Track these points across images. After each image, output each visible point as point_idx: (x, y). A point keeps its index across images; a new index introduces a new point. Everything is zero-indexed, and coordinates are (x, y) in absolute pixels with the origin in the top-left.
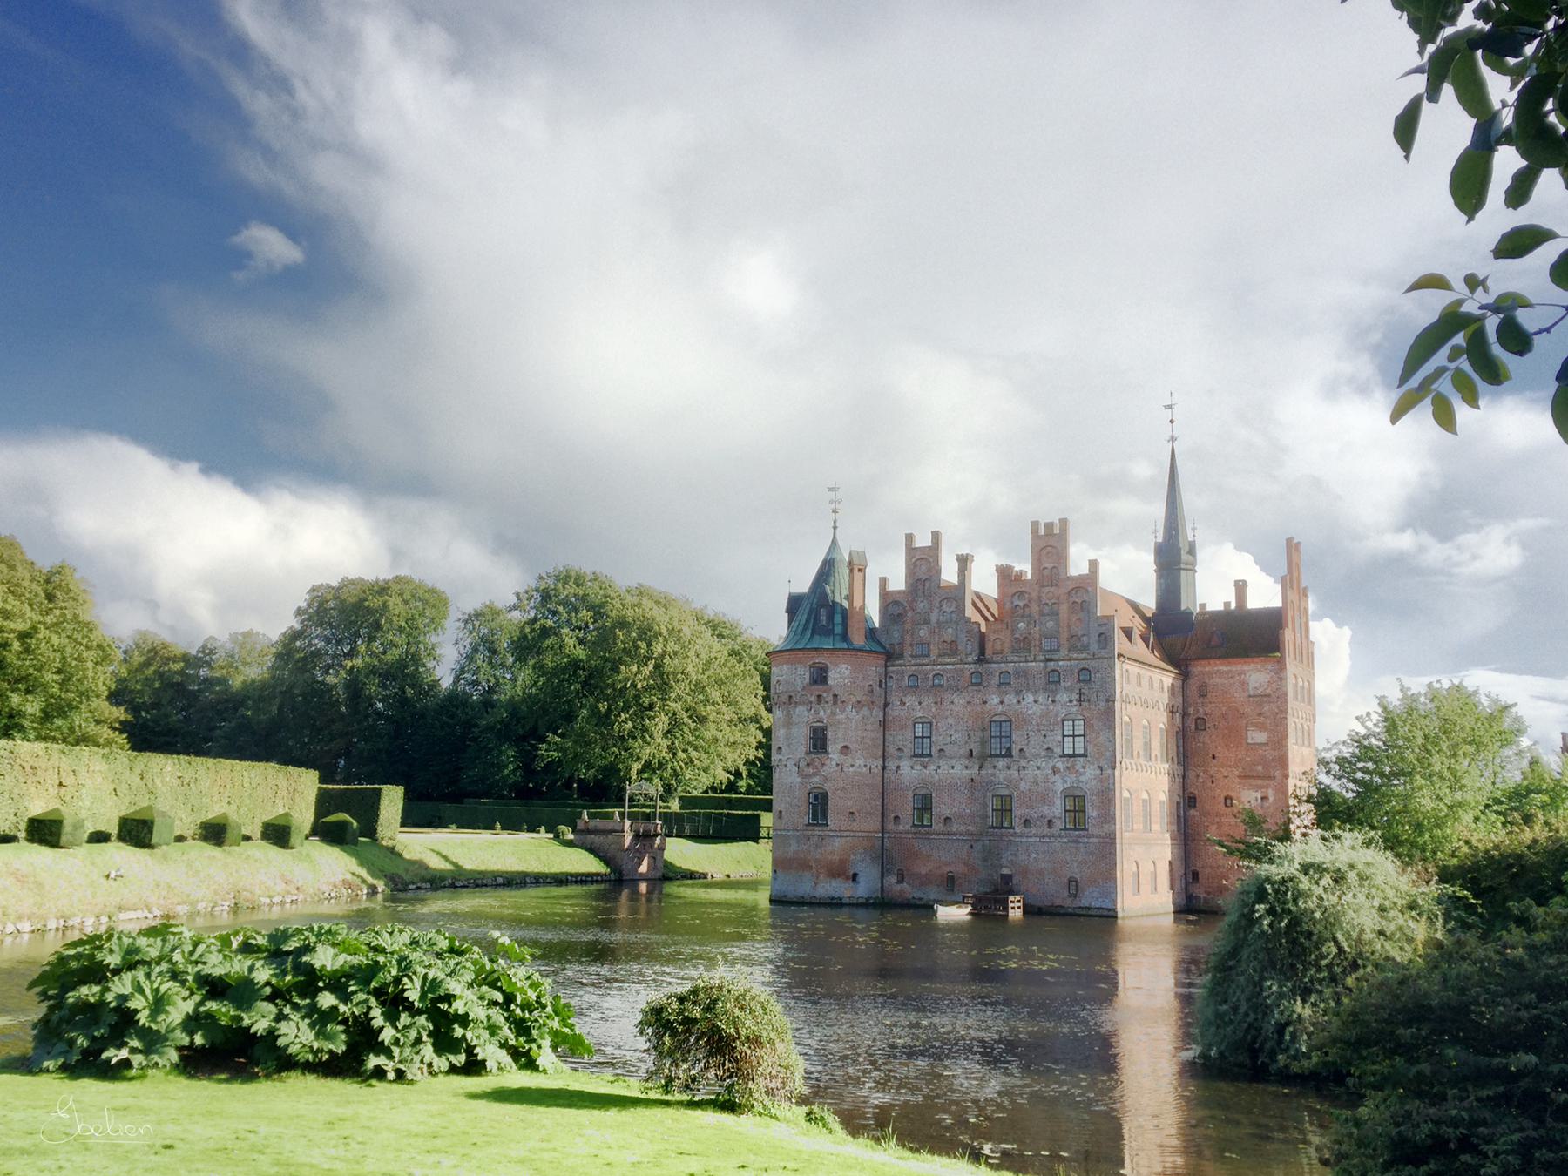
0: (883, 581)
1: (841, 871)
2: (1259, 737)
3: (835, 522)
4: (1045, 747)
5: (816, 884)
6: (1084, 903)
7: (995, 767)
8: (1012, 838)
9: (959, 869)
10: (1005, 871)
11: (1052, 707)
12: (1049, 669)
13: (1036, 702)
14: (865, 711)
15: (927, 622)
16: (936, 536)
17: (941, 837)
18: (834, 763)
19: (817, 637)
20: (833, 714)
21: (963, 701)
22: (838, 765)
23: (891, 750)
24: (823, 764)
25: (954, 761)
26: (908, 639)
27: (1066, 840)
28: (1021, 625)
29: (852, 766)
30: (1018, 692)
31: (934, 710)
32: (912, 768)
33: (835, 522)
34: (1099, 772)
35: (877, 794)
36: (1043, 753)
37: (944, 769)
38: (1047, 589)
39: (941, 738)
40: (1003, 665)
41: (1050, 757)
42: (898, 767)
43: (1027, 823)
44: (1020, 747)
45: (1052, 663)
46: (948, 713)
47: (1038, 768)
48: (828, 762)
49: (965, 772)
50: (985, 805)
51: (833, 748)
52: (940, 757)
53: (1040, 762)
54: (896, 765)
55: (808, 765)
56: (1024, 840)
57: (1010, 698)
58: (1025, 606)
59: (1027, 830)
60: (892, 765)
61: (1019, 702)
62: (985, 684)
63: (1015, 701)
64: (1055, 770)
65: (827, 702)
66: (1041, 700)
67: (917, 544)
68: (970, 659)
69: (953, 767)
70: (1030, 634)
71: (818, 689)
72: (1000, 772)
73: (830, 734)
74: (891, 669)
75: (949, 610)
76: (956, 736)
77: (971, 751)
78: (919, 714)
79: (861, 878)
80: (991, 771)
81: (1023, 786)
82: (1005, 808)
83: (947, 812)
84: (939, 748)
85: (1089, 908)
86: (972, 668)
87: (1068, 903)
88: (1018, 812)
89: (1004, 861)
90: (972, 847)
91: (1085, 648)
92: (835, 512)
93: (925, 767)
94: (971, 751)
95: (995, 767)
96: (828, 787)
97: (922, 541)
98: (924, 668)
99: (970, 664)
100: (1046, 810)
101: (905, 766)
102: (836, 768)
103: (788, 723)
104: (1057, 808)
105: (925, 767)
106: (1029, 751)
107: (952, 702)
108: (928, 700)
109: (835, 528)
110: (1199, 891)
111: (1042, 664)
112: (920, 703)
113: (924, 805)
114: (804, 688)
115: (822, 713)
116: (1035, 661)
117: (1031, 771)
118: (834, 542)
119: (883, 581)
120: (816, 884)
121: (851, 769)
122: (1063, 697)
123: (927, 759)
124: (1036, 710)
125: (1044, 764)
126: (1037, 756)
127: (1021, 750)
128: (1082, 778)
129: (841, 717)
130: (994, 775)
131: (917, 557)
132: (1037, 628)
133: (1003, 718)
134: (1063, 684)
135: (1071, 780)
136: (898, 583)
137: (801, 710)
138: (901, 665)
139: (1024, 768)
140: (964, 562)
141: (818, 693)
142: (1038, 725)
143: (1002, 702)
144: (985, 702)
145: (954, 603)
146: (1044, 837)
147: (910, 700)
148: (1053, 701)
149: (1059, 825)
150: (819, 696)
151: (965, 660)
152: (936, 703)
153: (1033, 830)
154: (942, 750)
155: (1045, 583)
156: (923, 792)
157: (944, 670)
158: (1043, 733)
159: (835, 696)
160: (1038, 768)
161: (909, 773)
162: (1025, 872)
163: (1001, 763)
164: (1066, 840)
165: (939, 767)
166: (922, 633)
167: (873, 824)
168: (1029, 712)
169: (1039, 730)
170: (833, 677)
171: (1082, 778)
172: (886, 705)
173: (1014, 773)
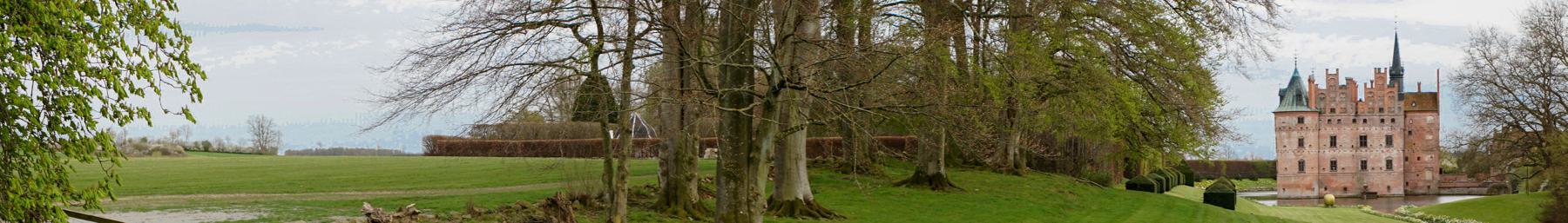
1: (1310, 188)
2: (1430, 137)
6: (1392, 193)
9: (1348, 185)
15: (1334, 101)
16: (1337, 70)
23: (1321, 145)
35: (1317, 160)
43: (1373, 169)
50: (1357, 164)
51: (1306, 146)
57: (1367, 128)
60: (1321, 151)
64: (1383, 151)
71: (1301, 125)
72: (1363, 152)
73: (1305, 141)
82: (1364, 165)
83: (1342, 166)
87: (1388, 194)
88: (1369, 165)
96: (1305, 159)
103: (1289, 137)
104: (1384, 164)
106: (1374, 145)
110: (1409, 189)
113: (1334, 164)
117: (1375, 152)
118: (1296, 71)
122: (1385, 128)
124: (1376, 132)
135: (1388, 155)
137: (1295, 132)
149: (1384, 169)
161: (1329, 153)
162: (1372, 184)
163: (1364, 149)
167: (1316, 171)
170: (1306, 121)
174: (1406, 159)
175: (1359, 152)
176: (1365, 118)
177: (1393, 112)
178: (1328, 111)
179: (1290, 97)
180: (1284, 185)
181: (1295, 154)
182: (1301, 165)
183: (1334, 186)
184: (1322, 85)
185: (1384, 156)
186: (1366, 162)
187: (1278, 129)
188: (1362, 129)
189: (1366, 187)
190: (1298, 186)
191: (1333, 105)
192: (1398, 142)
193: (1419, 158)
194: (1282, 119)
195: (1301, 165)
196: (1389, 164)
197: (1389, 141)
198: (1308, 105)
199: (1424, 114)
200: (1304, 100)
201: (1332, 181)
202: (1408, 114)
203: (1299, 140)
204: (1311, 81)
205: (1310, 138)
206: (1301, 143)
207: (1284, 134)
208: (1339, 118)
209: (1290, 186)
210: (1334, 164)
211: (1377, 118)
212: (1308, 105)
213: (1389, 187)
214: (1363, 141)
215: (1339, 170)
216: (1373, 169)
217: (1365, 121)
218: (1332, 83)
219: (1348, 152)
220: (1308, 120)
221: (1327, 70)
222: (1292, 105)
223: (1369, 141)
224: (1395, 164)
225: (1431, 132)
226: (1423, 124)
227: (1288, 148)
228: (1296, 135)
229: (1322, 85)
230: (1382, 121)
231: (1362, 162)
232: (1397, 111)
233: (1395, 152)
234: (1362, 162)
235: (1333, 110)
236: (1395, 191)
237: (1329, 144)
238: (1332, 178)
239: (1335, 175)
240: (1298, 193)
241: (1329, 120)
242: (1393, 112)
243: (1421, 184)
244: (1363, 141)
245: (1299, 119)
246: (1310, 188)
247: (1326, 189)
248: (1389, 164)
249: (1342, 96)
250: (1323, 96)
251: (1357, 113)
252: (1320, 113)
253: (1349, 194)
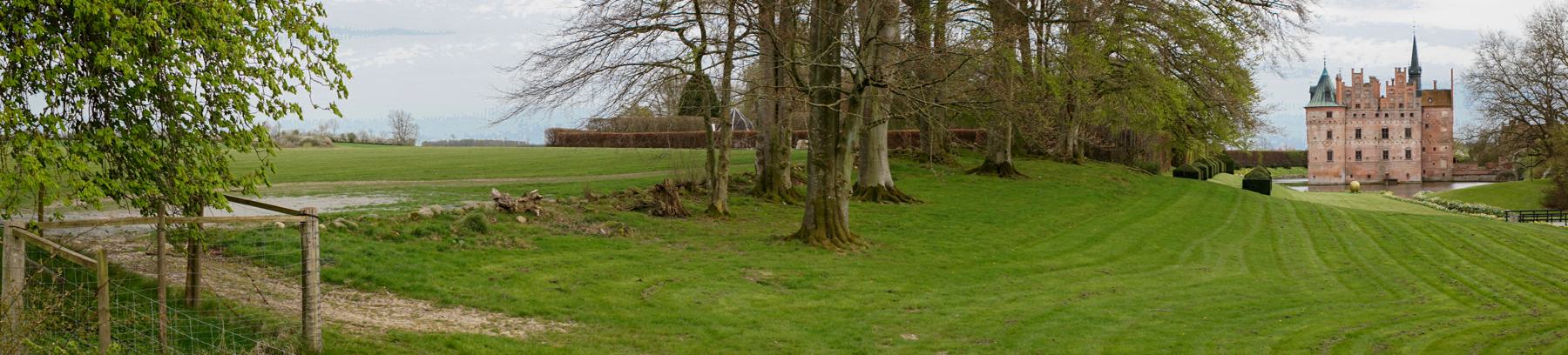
1: (1337, 175)
2: (1445, 130)
9: (1371, 173)
23: (1348, 137)
35: (1343, 151)
43: (1394, 158)
51: (1334, 137)
57: (1388, 122)
60: (1348, 142)
67: (1355, 72)
71: (1330, 119)
72: (1385, 144)
73: (1333, 133)
82: (1386, 155)
83: (1367, 156)
87: (1407, 181)
88: (1390, 155)
91: (1412, 107)
96: (1333, 149)
97: (1357, 71)
101: (1353, 143)
103: (1319, 130)
104: (1404, 154)
106: (1395, 137)
108: (1361, 122)
110: (1426, 176)
113: (1359, 154)
118: (1325, 70)
122: (1405, 122)
124: (1397, 125)
137: (1324, 126)
149: (1404, 158)
161: (1355, 144)
162: (1393, 172)
163: (1385, 141)
167: (1343, 160)
174: (1423, 149)
177: (1412, 107)
178: (1354, 106)
179: (1319, 94)
180: (1314, 173)
182: (1330, 155)
184: (1349, 84)
185: (1404, 147)
187: (1309, 123)
188: (1384, 123)
189: (1387, 175)
190: (1327, 174)
191: (1358, 101)
192: (1416, 134)
193: (1435, 149)
194: (1312, 113)
195: (1330, 155)
196: (1408, 153)
197: (1408, 133)
198: (1335, 101)
199: (1438, 109)
200: (1332, 96)
201: (1356, 169)
202: (1425, 109)
203: (1328, 132)
204: (1338, 79)
205: (1338, 130)
206: (1329, 135)
207: (1314, 127)
209: (1319, 174)
210: (1359, 154)
211: (1397, 113)
212: (1335, 101)
214: (1385, 133)
215: (1363, 160)
216: (1394, 158)
217: (1387, 115)
218: (1357, 81)
220: (1336, 114)
221: (1353, 70)
223: (1390, 133)
224: (1413, 154)
225: (1445, 126)
226: (1438, 118)
227: (1318, 140)
228: (1325, 128)
229: (1349, 84)
230: (1402, 115)
231: (1384, 152)
232: (1415, 107)
233: (1414, 143)
234: (1384, 152)
235: (1358, 106)
236: (1413, 179)
237: (1354, 136)
238: (1357, 166)
239: (1360, 164)
240: (1327, 180)
241: (1355, 115)
243: (1436, 172)
244: (1385, 133)
245: (1328, 113)
246: (1337, 175)
247: (1352, 176)
248: (1408, 153)
250: (1348, 93)
251: (1379, 108)
252: (1347, 108)
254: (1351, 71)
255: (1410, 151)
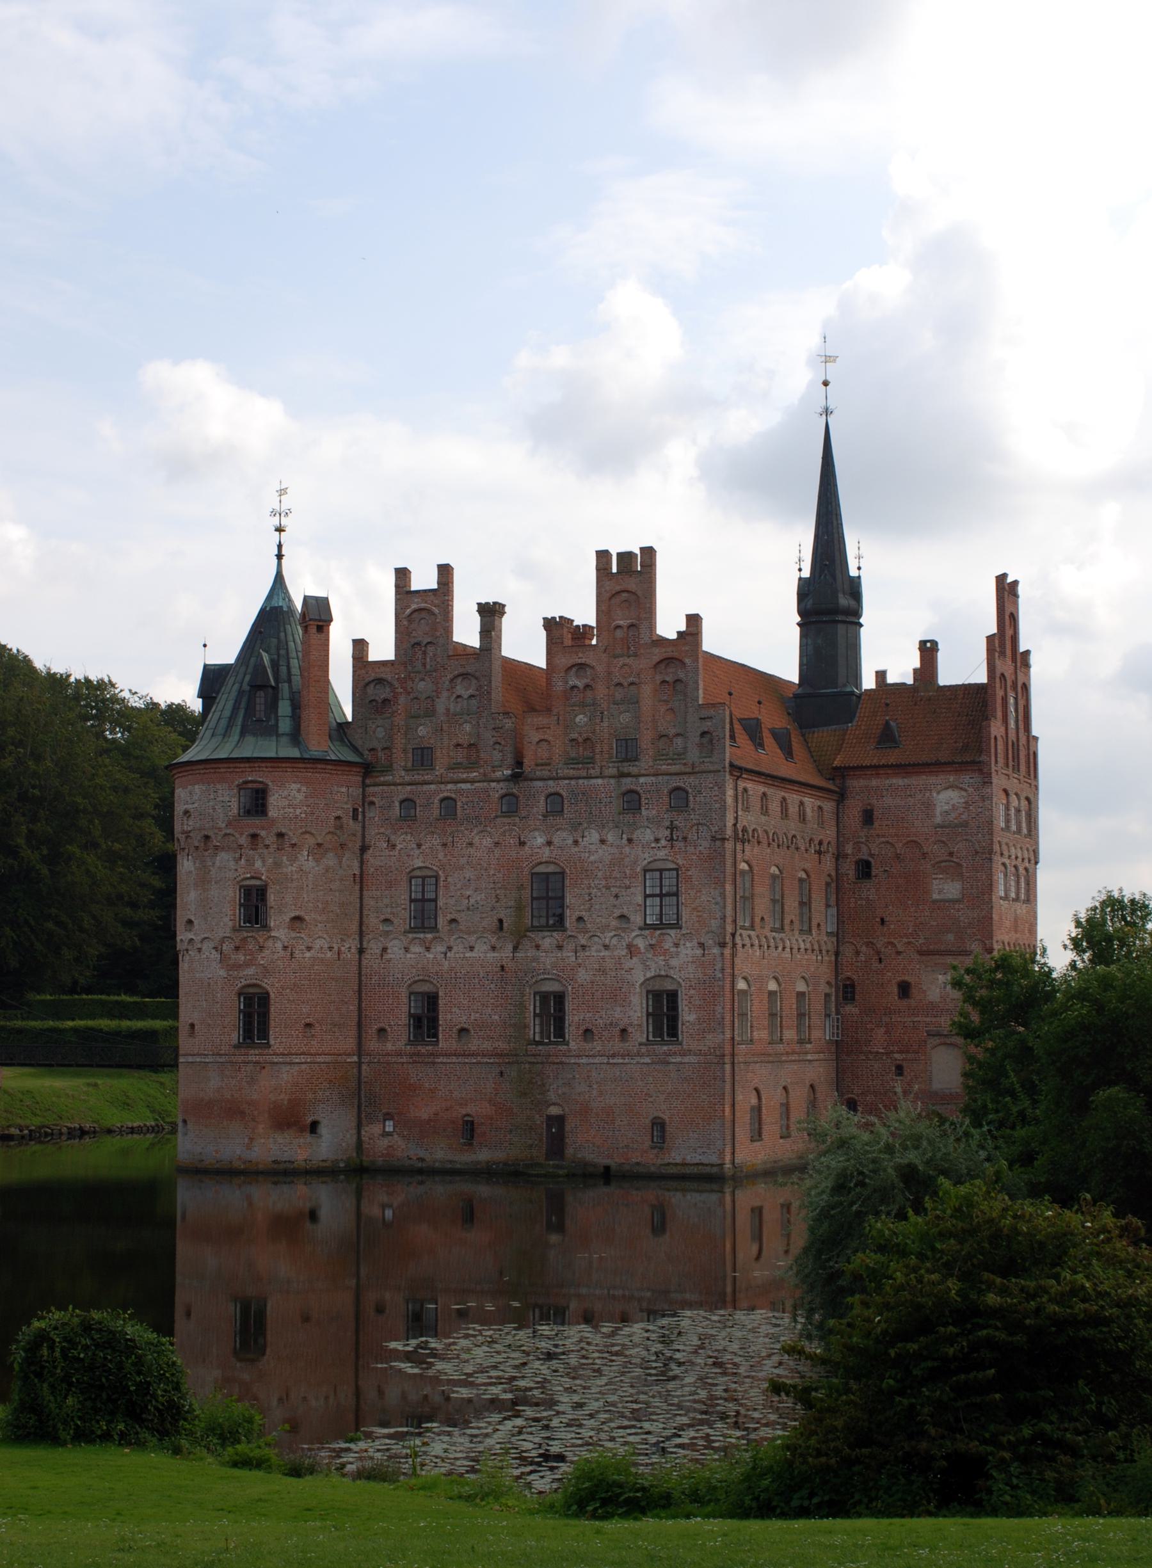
0: (360, 646)
2: (947, 889)
3: (280, 546)
4: (617, 913)
5: (251, 1139)
6: (676, 1157)
7: (538, 947)
8: (564, 1059)
9: (478, 1110)
10: (554, 1111)
11: (627, 850)
12: (624, 789)
13: (603, 841)
14: (330, 860)
15: (431, 713)
16: (445, 572)
17: (454, 1059)
18: (279, 945)
19: (250, 739)
20: (277, 865)
21: (488, 842)
22: (285, 948)
23: (372, 920)
24: (261, 948)
25: (473, 938)
26: (399, 741)
27: (647, 1060)
28: (580, 719)
29: (309, 949)
30: (575, 827)
31: (441, 856)
32: (407, 950)
33: (280, 546)
34: (699, 952)
36: (614, 923)
37: (458, 948)
38: (622, 661)
39: (452, 901)
40: (551, 783)
41: (624, 930)
42: (385, 950)
44: (577, 914)
45: (628, 780)
46: (463, 861)
47: (606, 947)
48: (270, 943)
49: (491, 955)
50: (522, 1006)
51: (278, 922)
52: (451, 932)
53: (607, 937)
54: (381, 946)
55: (237, 948)
56: (584, 1060)
57: (563, 837)
58: (587, 686)
59: (588, 1046)
60: (374, 948)
61: (576, 842)
62: (523, 813)
63: (570, 842)
64: (632, 950)
65: (267, 847)
66: (610, 838)
67: (416, 585)
68: (498, 774)
69: (472, 948)
70: (594, 732)
73: (271, 898)
74: (371, 789)
75: (466, 694)
76: (477, 898)
77: (501, 921)
78: (418, 863)
79: (323, 1130)
80: (531, 953)
81: (583, 976)
84: (449, 917)
85: (684, 1164)
86: (498, 789)
87: (651, 1160)
88: (574, 1017)
89: (552, 1096)
90: (501, 1073)
92: (280, 530)
93: (428, 949)
94: (501, 921)
95: (538, 947)
96: (271, 985)
97: (424, 580)
98: (426, 787)
99: (498, 781)
100: (617, 1013)
101: (395, 949)
102: (282, 953)
104: (636, 1010)
105: (428, 949)
107: (471, 844)
108: (436, 841)
109: (280, 556)
111: (612, 781)
112: (419, 846)
114: (229, 824)
115: (258, 864)
116: (601, 776)
118: (279, 579)
119: (360, 646)
120: (251, 1139)
121: (308, 955)
123: (429, 936)
125: (614, 941)
126: (605, 928)
127: (580, 919)
128: (674, 962)
129: (290, 869)
130: (535, 959)
131: (414, 606)
132: (605, 724)
133: (551, 869)
134: (644, 812)
135: (656, 965)
136: (383, 649)
137: (223, 857)
138: (389, 784)
139: (584, 947)
140: (491, 613)
141: (251, 831)
142: (606, 878)
143: (549, 843)
144: (522, 844)
145: (474, 681)
146: (613, 1056)
147: (403, 841)
148: (630, 841)
149: (639, 1036)
150: (254, 836)
151: (493, 776)
152: (445, 845)
153: (598, 1046)
154: (453, 921)
155: (618, 651)
156: (426, 988)
157: (456, 791)
158: (614, 890)
159: (280, 835)
160: (606, 947)
163: (548, 940)
164: (647, 1060)
165: (450, 948)
166: (422, 731)
168: (592, 858)
169: (608, 888)
170: (276, 803)
171: (674, 962)
172: (364, 849)
173: (568, 954)
174: (847, 991)
175: (527, 952)
176: (552, 786)
177: (681, 755)
178: (400, 759)
181: (223, 958)
183: (424, 1113)
186: (560, 998)
193: (905, 989)
200: (284, 708)
202: (855, 784)
203: (247, 891)
208: (448, 790)
211: (603, 786)
212: (295, 737)
213: (659, 1125)
215: (447, 1041)
218: (420, 633)
219: (481, 950)
222: (226, 734)
225: (951, 867)
230: (632, 801)
231: (544, 997)
232: (693, 755)
233: (689, 950)
235: (423, 757)
237: (403, 917)
241: (407, 802)
242: (681, 755)
249: (460, 690)
251: (519, 763)
253: (483, 1155)
254: (390, 580)
255: (673, 996)
